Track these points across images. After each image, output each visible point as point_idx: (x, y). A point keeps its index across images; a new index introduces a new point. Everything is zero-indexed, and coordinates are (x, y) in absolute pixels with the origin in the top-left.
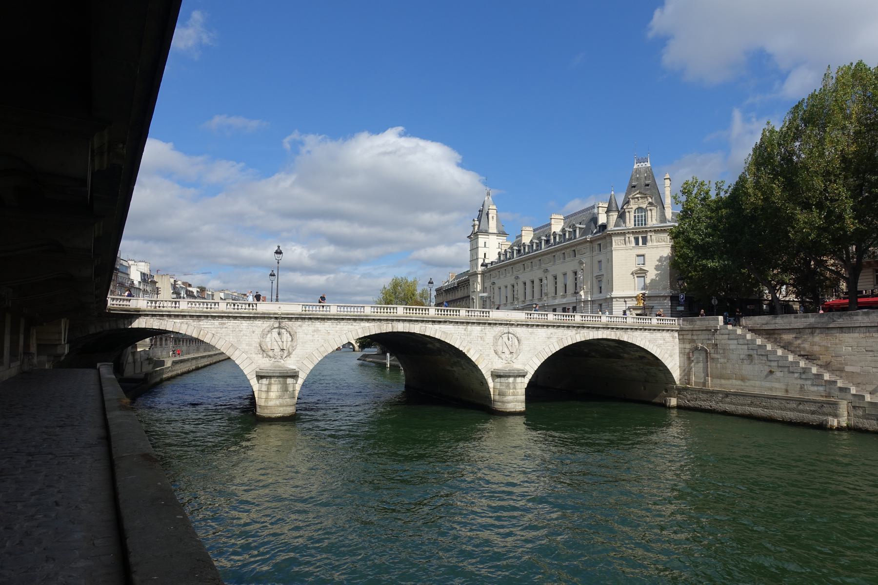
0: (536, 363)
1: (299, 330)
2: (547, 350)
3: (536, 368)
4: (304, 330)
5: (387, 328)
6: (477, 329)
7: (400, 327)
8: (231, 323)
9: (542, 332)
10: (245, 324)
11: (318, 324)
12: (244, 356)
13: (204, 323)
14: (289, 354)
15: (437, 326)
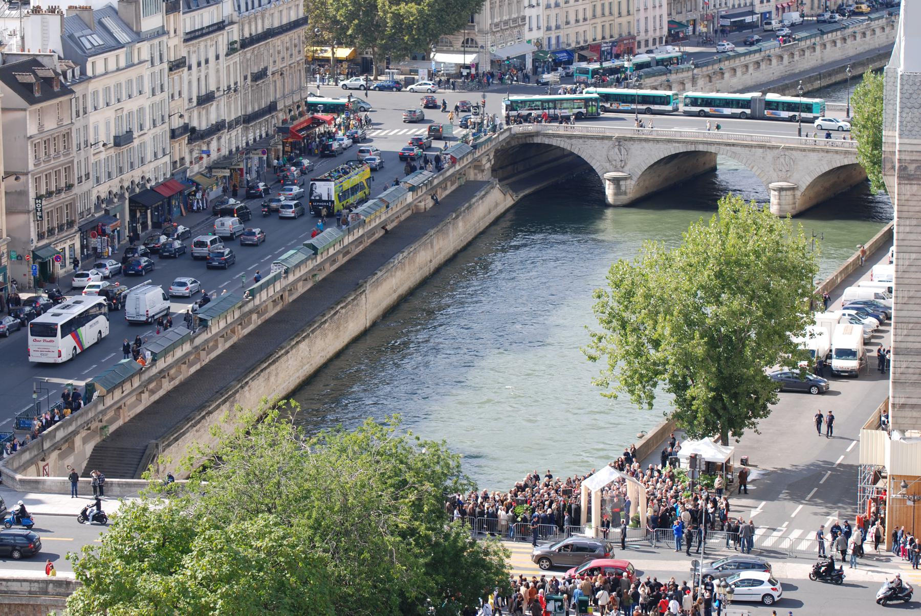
0: (808, 180)
1: (632, 147)
2: (818, 170)
3: (808, 183)
4: (635, 148)
5: (691, 148)
6: (761, 150)
7: (701, 148)
8: (589, 142)
9: (814, 156)
10: (598, 142)
11: (644, 144)
12: (598, 163)
13: (574, 141)
14: (626, 164)
15: (728, 148)
